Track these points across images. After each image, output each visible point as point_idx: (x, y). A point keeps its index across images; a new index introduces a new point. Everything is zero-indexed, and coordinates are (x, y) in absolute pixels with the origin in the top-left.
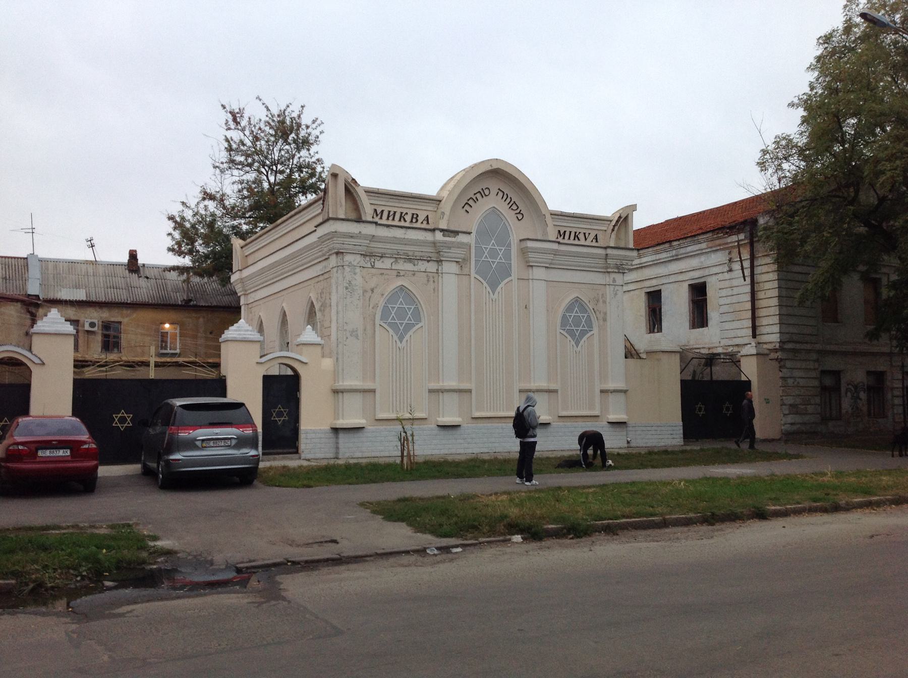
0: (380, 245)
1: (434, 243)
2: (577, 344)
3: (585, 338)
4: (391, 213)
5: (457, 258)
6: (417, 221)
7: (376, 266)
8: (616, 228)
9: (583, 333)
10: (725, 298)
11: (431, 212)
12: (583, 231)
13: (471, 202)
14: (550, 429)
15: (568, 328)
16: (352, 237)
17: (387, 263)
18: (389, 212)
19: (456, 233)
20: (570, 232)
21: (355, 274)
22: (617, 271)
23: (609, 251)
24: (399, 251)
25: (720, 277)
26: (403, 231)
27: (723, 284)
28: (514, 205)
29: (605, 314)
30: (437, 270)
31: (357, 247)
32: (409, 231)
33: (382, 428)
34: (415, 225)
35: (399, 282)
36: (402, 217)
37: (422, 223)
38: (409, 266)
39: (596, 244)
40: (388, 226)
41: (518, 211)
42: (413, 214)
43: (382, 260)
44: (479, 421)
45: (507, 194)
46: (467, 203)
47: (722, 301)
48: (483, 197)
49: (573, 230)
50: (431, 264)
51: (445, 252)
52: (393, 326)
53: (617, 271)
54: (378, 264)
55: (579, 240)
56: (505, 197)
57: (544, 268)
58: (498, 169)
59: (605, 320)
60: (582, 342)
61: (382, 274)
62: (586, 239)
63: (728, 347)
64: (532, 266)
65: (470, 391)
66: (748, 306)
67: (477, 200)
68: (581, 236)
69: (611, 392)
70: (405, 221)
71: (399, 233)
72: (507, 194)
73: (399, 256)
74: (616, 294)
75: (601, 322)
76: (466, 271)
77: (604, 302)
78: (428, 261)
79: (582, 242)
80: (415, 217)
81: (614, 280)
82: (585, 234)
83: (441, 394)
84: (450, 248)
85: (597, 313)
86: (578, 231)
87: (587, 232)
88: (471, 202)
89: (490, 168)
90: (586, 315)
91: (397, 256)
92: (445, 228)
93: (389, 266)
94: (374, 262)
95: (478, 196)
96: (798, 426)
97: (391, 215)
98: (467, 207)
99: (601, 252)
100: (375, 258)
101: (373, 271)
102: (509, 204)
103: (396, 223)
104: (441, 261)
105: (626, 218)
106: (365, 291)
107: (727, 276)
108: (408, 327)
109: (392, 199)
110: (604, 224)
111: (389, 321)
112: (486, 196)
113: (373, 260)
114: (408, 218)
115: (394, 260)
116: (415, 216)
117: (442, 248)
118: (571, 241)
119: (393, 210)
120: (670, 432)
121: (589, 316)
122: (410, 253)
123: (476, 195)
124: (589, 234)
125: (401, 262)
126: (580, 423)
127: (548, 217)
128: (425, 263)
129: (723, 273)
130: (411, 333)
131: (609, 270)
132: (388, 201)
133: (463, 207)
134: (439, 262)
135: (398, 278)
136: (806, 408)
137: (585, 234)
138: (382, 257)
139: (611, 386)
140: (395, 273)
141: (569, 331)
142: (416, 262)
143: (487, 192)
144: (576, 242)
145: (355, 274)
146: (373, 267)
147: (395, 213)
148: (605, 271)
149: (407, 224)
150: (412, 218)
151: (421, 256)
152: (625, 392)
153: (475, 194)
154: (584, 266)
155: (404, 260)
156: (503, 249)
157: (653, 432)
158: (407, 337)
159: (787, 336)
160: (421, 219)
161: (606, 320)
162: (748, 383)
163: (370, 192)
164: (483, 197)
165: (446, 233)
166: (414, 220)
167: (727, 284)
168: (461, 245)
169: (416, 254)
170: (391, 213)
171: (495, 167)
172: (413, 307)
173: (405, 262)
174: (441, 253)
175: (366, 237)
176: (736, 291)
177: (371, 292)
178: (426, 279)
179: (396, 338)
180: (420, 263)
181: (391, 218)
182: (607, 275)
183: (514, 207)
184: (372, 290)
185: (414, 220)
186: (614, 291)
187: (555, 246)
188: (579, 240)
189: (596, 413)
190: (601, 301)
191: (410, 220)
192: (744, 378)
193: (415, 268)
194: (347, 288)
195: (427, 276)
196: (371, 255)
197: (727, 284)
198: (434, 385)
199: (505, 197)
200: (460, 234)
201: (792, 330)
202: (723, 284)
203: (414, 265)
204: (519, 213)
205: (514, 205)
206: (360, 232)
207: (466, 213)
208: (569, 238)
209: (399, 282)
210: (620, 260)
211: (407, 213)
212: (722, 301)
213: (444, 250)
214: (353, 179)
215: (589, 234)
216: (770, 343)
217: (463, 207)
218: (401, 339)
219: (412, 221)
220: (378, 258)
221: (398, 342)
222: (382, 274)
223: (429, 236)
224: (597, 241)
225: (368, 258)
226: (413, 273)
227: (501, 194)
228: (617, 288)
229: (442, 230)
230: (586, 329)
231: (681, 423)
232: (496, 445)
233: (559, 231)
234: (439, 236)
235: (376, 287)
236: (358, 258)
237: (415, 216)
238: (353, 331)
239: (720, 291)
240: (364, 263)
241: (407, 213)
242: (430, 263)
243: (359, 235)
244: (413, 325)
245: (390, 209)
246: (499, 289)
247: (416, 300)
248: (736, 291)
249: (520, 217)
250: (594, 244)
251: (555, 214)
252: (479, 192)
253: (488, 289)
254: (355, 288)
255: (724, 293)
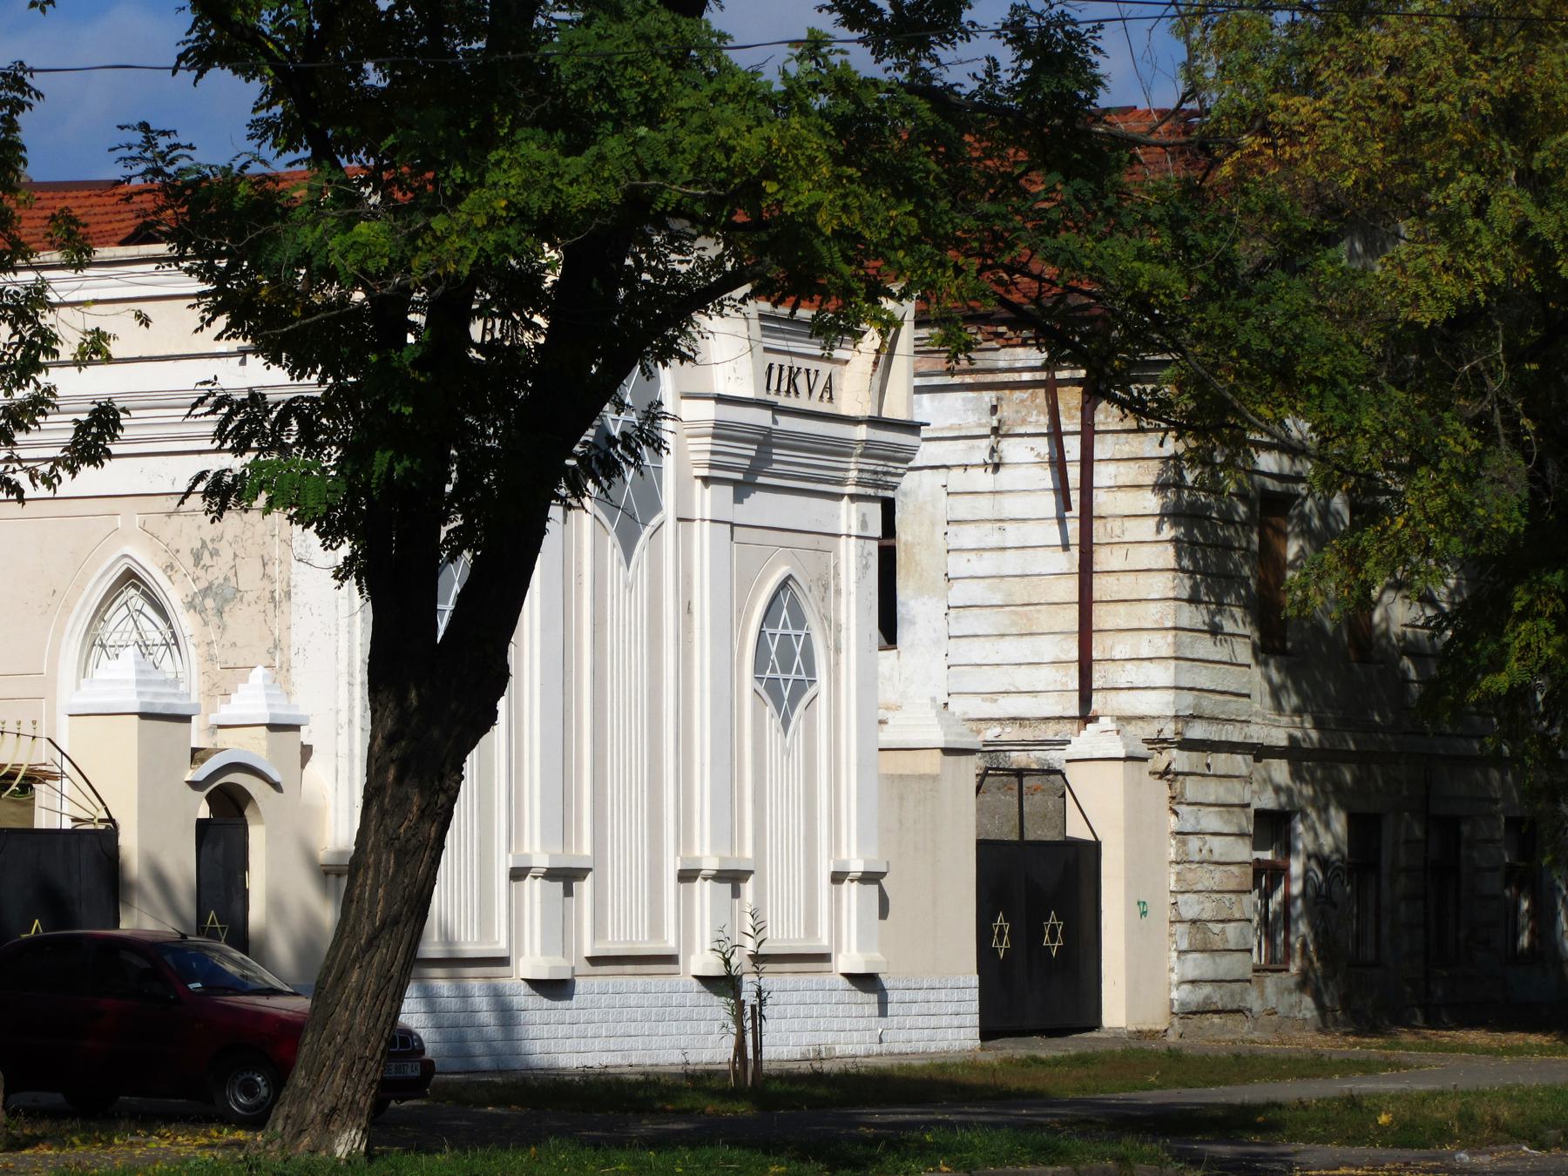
10: (972, 556)
20: (781, 367)
25: (956, 479)
27: (962, 508)
47: (958, 565)
60: (794, 720)
63: (983, 725)
66: (1069, 589)
82: (808, 371)
86: (799, 363)
96: (1207, 990)
107: (984, 480)
120: (951, 1008)
129: (966, 467)
136: (1223, 931)
137: (808, 371)
157: (924, 1008)
159: (1189, 698)
162: (1090, 852)
167: (984, 507)
176: (1013, 534)
187: (763, 418)
192: (1076, 829)
197: (984, 507)
201: (1204, 677)
202: (962, 508)
208: (778, 390)
212: (958, 565)
216: (1142, 718)
231: (974, 980)
239: (952, 529)
248: (1013, 534)
255: (968, 536)
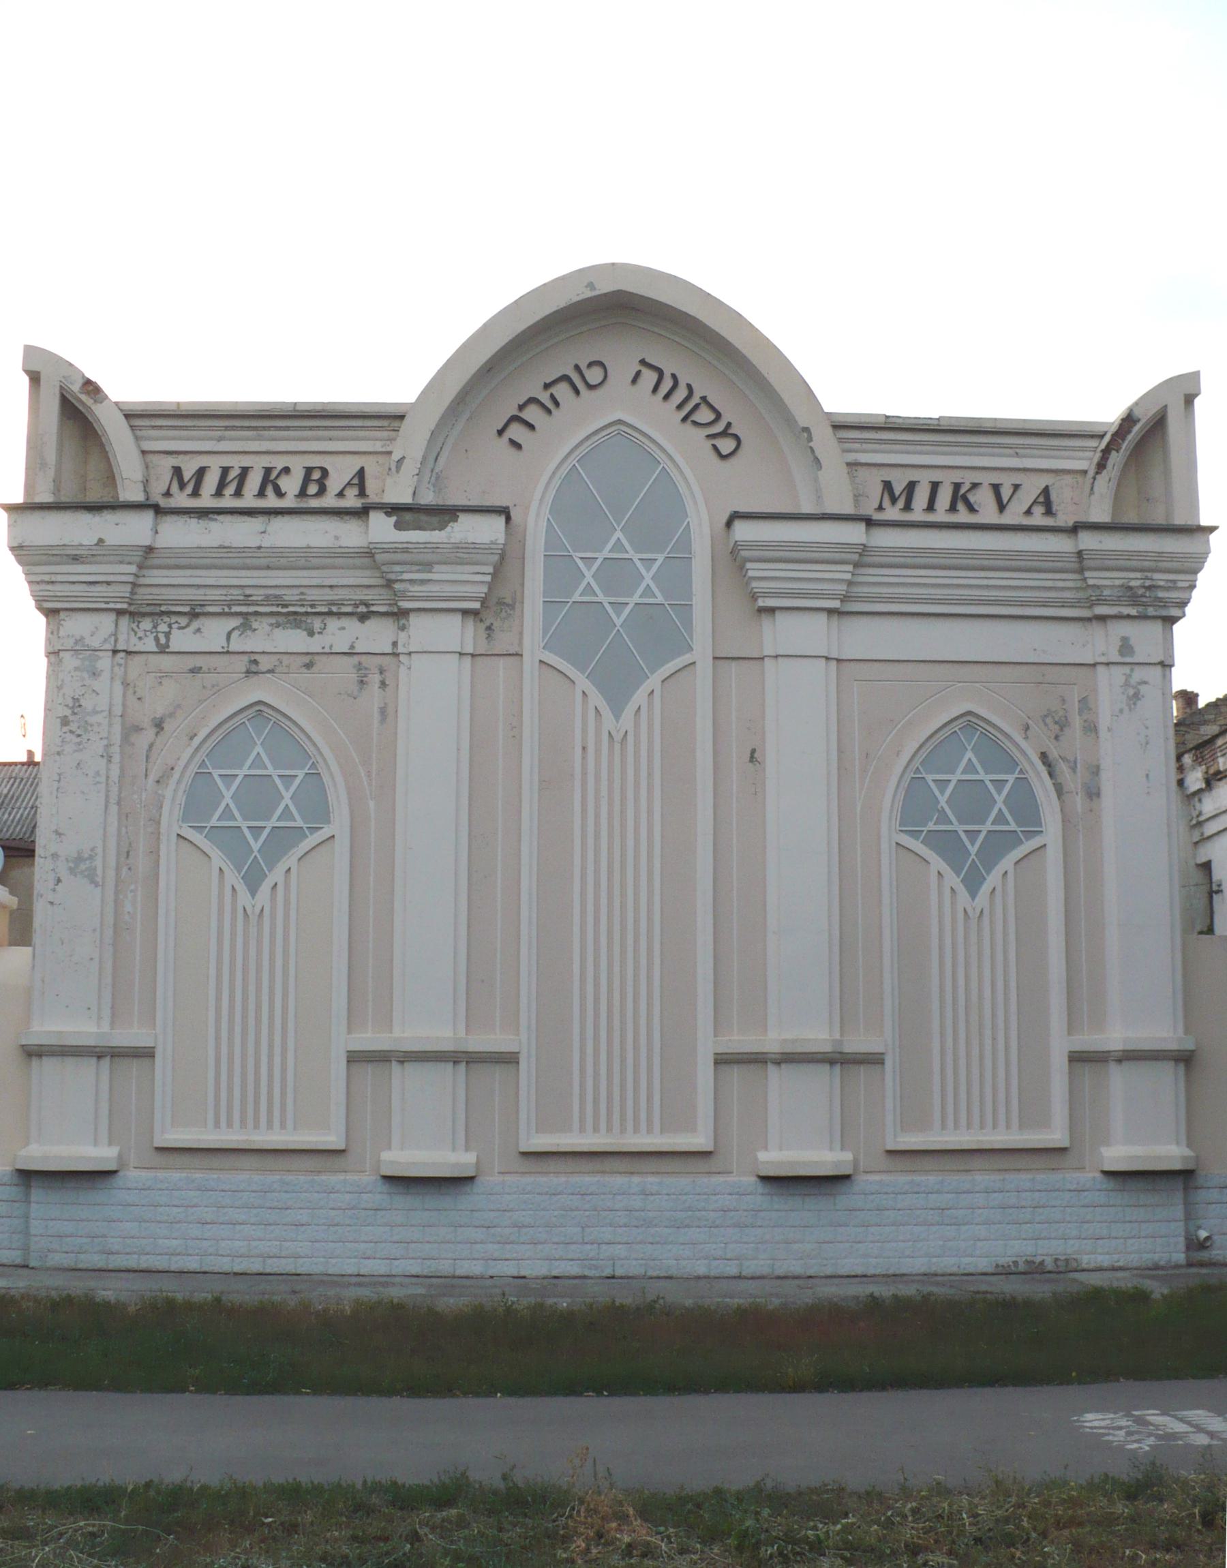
0: (179, 577)
1: (369, 553)
2: (973, 883)
3: (1007, 863)
4: (233, 474)
5: (464, 599)
6: (322, 491)
7: (174, 646)
8: (1116, 459)
9: (999, 844)
11: (372, 459)
12: (987, 479)
13: (531, 414)
14: (845, 1199)
15: (931, 826)
16: (76, 559)
17: (213, 634)
18: (225, 471)
19: (446, 514)
20: (935, 486)
21: (95, 674)
22: (1133, 611)
23: (1088, 541)
24: (248, 592)
26: (256, 523)
28: (703, 408)
29: (1096, 771)
30: (395, 644)
31: (98, 588)
32: (278, 523)
33: (176, 1176)
34: (314, 503)
35: (256, 691)
36: (269, 481)
37: (341, 494)
38: (293, 640)
39: (1048, 522)
40: (203, 513)
41: (719, 428)
42: (309, 471)
43: (196, 624)
44: (552, 1165)
45: (674, 376)
46: (515, 419)
48: (577, 392)
49: (947, 480)
50: (372, 624)
51: (411, 581)
52: (229, 838)
53: (1133, 611)
54: (182, 640)
55: (971, 509)
56: (667, 384)
57: (823, 617)
58: (619, 294)
59: (1093, 793)
60: (993, 879)
61: (195, 671)
62: (1002, 507)
64: (772, 610)
65: (509, 1060)
67: (557, 404)
68: (984, 499)
69: (1119, 1061)
70: (280, 494)
71: (242, 533)
72: (674, 376)
73: (251, 609)
74: (1137, 696)
75: (1078, 802)
76: (504, 642)
77: (1091, 728)
78: (363, 618)
79: (989, 513)
80: (316, 479)
81: (1126, 647)
82: (996, 488)
83: (394, 1063)
84: (428, 566)
85: (1063, 768)
86: (968, 478)
87: (1007, 482)
88: (531, 414)
89: (589, 294)
90: (1011, 778)
91: (244, 609)
92: (407, 499)
93: (218, 644)
94: (168, 635)
95: (562, 391)
97: (237, 480)
98: (516, 431)
99: (1060, 544)
100: (174, 619)
101: (166, 662)
102: (680, 407)
103: (249, 500)
104: (405, 613)
105: (1159, 423)
106: (131, 730)
108: (282, 840)
109: (234, 428)
110: (1083, 449)
111: (214, 822)
112: (591, 387)
113: (163, 628)
114: (291, 485)
115: (235, 622)
116: (316, 475)
117: (397, 568)
118: (941, 515)
119: (236, 463)
121: (1022, 781)
122: (290, 596)
123: (554, 390)
124: (1016, 487)
125: (262, 625)
126: (978, 1177)
127: (824, 441)
128: (352, 625)
130: (290, 860)
131: (1100, 610)
132: (220, 439)
133: (500, 432)
134: (398, 615)
135: (255, 679)
137: (996, 488)
138: (194, 615)
139: (1115, 1037)
140: (241, 664)
141: (932, 840)
142: (317, 623)
143: (594, 376)
144: (963, 516)
145: (95, 674)
146: (163, 650)
147: (245, 471)
148: (1085, 613)
149: (289, 502)
150: (307, 480)
151: (332, 603)
152: (1185, 1059)
153: (547, 386)
154: (1023, 604)
155: (273, 620)
156: (660, 558)
158: (276, 875)
160: (334, 485)
161: (1098, 795)
163: (135, 416)
164: (577, 392)
165: (408, 516)
166: (313, 489)
168: (464, 554)
169: (313, 595)
170: (233, 474)
171: (605, 287)
172: (301, 774)
173: (278, 625)
174: (397, 586)
175: (119, 553)
177: (153, 731)
178: (354, 677)
179: (233, 878)
180: (333, 624)
181: (230, 490)
182: (1097, 630)
183: (704, 415)
184: (159, 725)
185: (313, 489)
186: (1127, 684)
187: (855, 534)
188: (971, 509)
189: (1056, 1136)
190: (1077, 722)
191: (297, 492)
193: (315, 645)
194: (65, 721)
195: (359, 666)
196: (158, 613)
198: (369, 1039)
199: (667, 384)
200: (463, 518)
203: (311, 633)
204: (724, 434)
205: (703, 408)
206: (101, 541)
207: (513, 451)
209: (256, 691)
210: (1141, 570)
211: (286, 470)
213: (406, 576)
214: (88, 382)
215: (1016, 487)
217: (500, 432)
218: (253, 882)
219: (302, 493)
220: (183, 621)
221: (242, 889)
222: (195, 671)
223: (350, 534)
224: (1049, 512)
225: (146, 624)
226: (307, 659)
227: (649, 377)
228: (1139, 674)
229: (392, 509)
230: (1013, 826)
232: (620, 1250)
233: (888, 486)
234: (381, 528)
235: (172, 715)
236: (106, 622)
237: (316, 475)
238: (79, 859)
240: (134, 640)
241: (286, 470)
242: (368, 623)
243: (100, 551)
244: (299, 833)
245: (226, 461)
246: (639, 697)
247: (311, 749)
249: (726, 445)
250: (1038, 518)
251: (842, 426)
252: (565, 378)
253: (596, 699)
254: (92, 719)
